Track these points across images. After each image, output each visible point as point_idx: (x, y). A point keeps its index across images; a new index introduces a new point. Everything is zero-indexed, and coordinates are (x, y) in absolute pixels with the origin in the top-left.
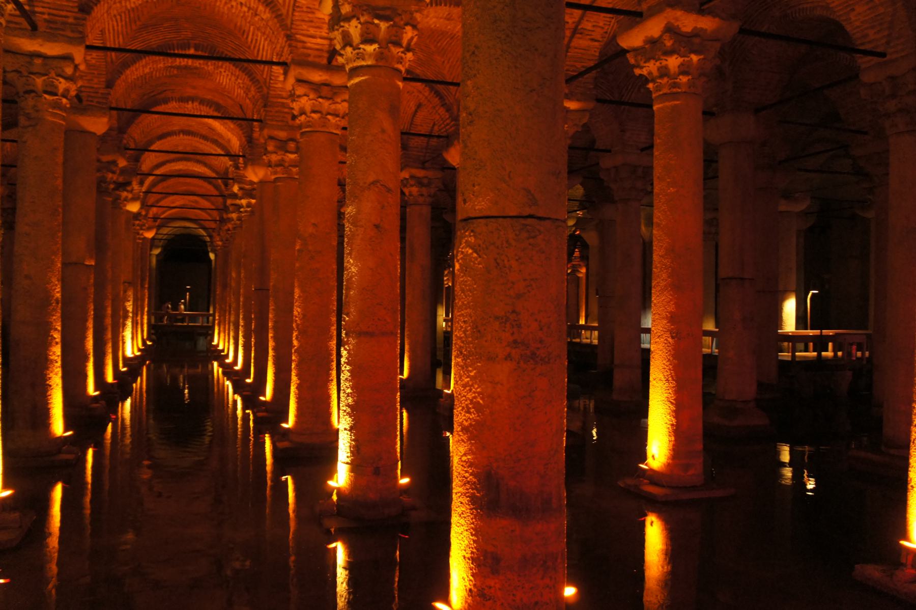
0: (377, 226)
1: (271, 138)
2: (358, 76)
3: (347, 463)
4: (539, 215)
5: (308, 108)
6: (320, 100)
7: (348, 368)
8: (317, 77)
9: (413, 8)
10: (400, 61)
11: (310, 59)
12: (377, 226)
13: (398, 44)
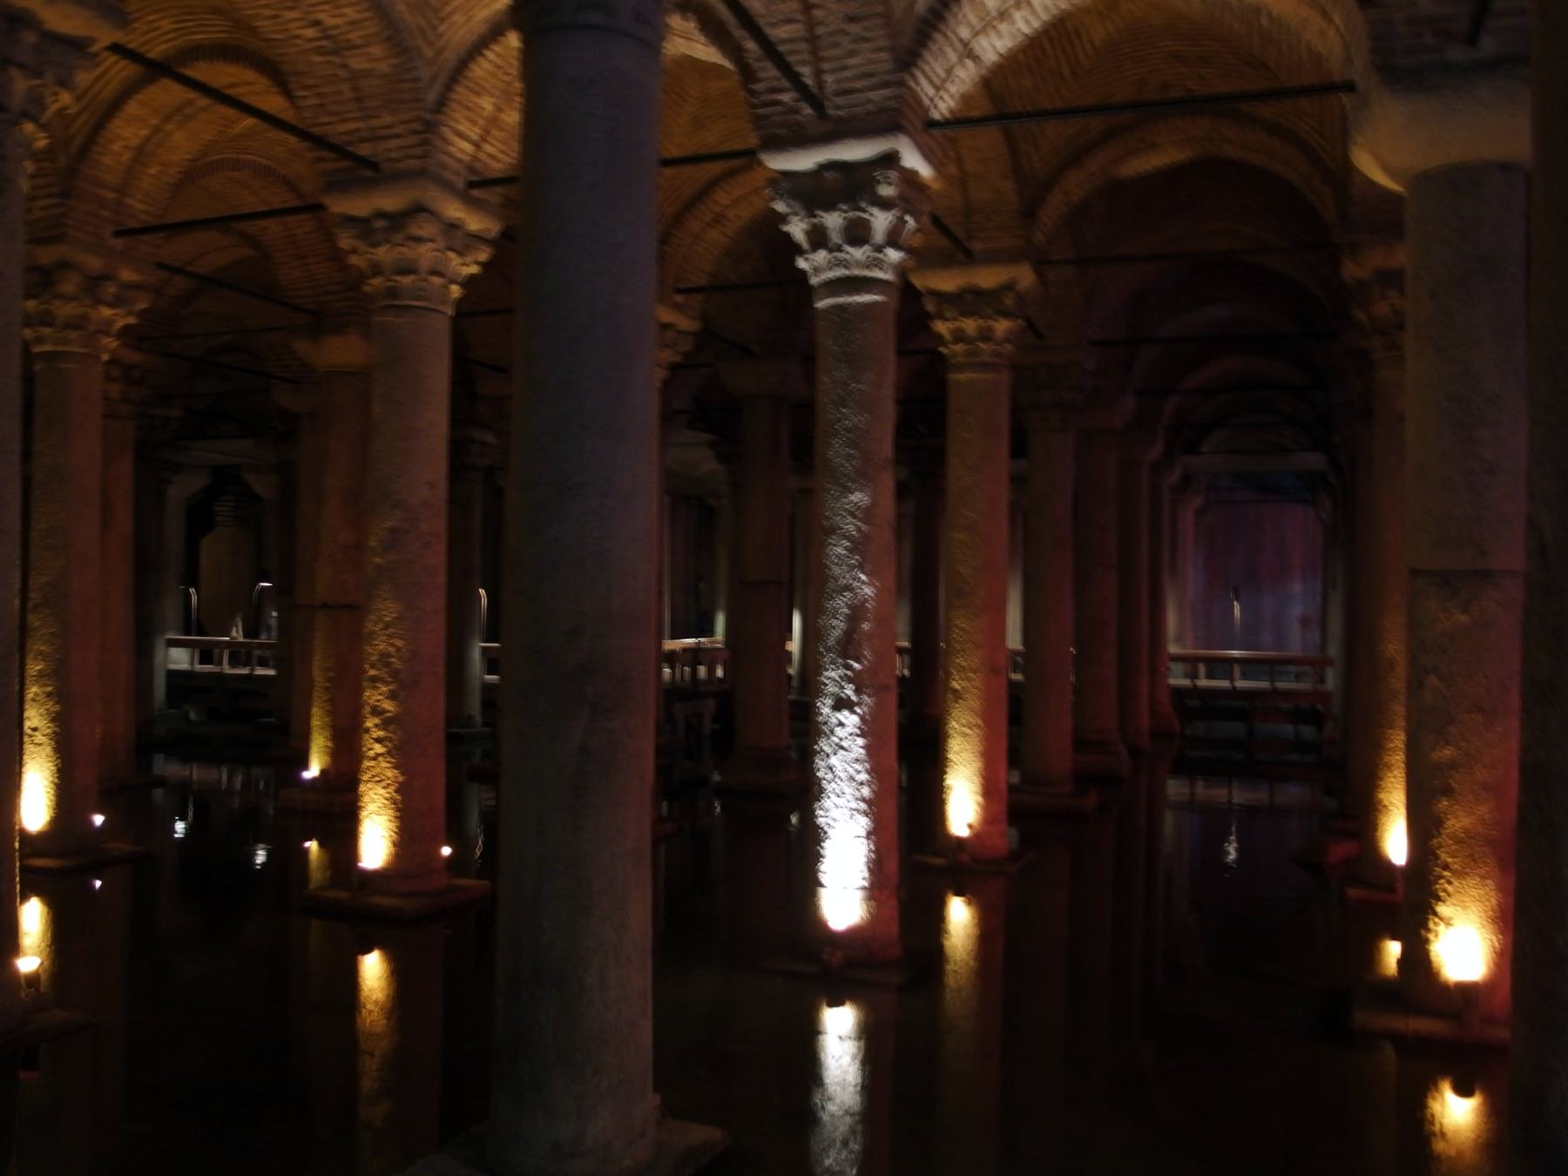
1: (65, 265)
2: (869, 292)
3: (864, 888)
5: (425, 265)
6: (451, 255)
7: (860, 741)
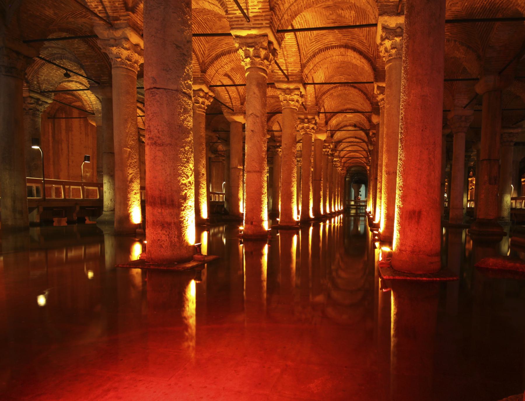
0: (252, 131)
4: (158, 87)
5: (283, 100)
8: (284, 86)
9: (262, 40)
10: (261, 64)
11: (281, 79)
12: (252, 131)
13: (259, 57)
